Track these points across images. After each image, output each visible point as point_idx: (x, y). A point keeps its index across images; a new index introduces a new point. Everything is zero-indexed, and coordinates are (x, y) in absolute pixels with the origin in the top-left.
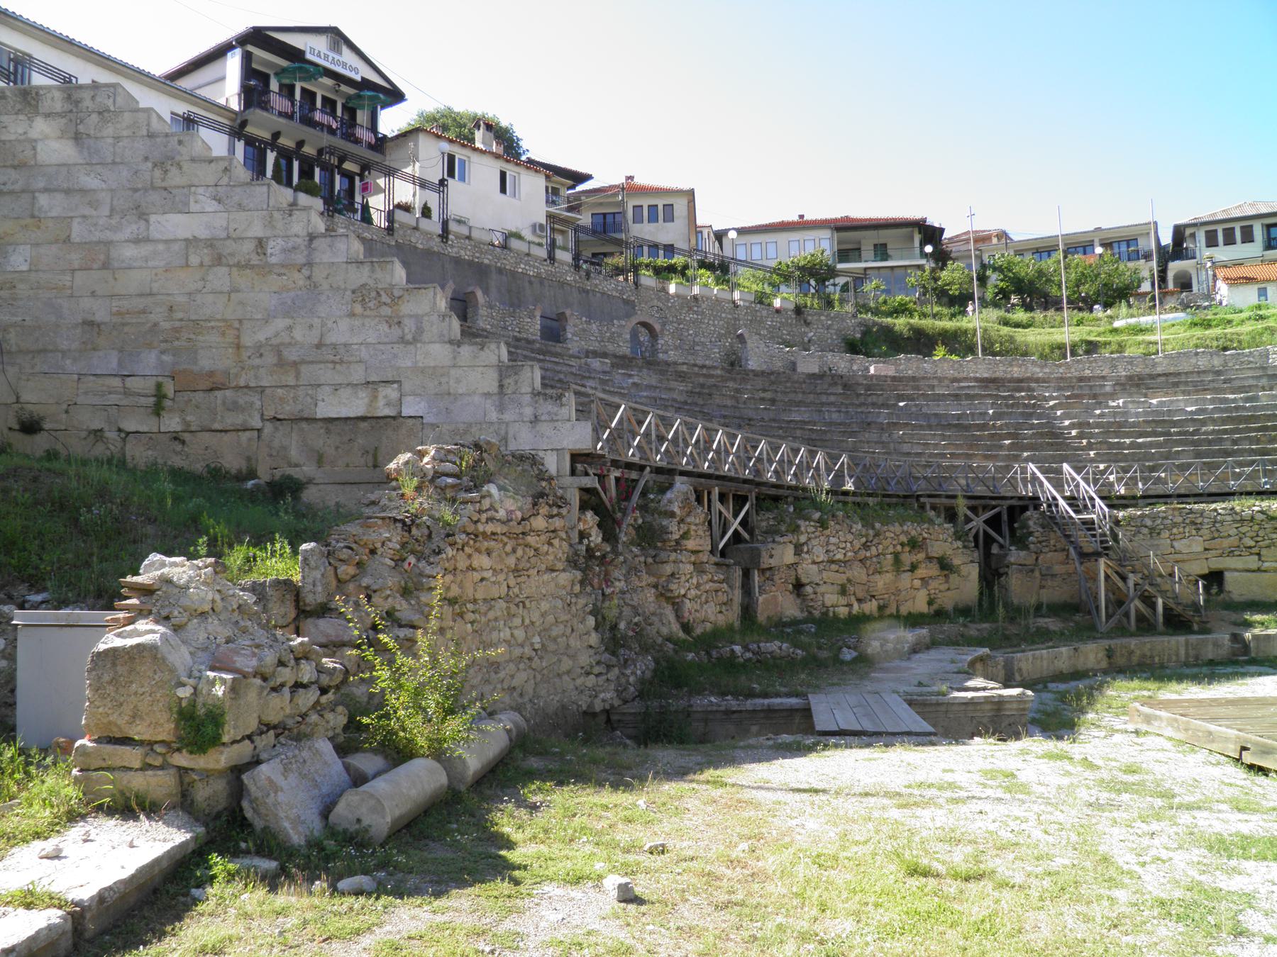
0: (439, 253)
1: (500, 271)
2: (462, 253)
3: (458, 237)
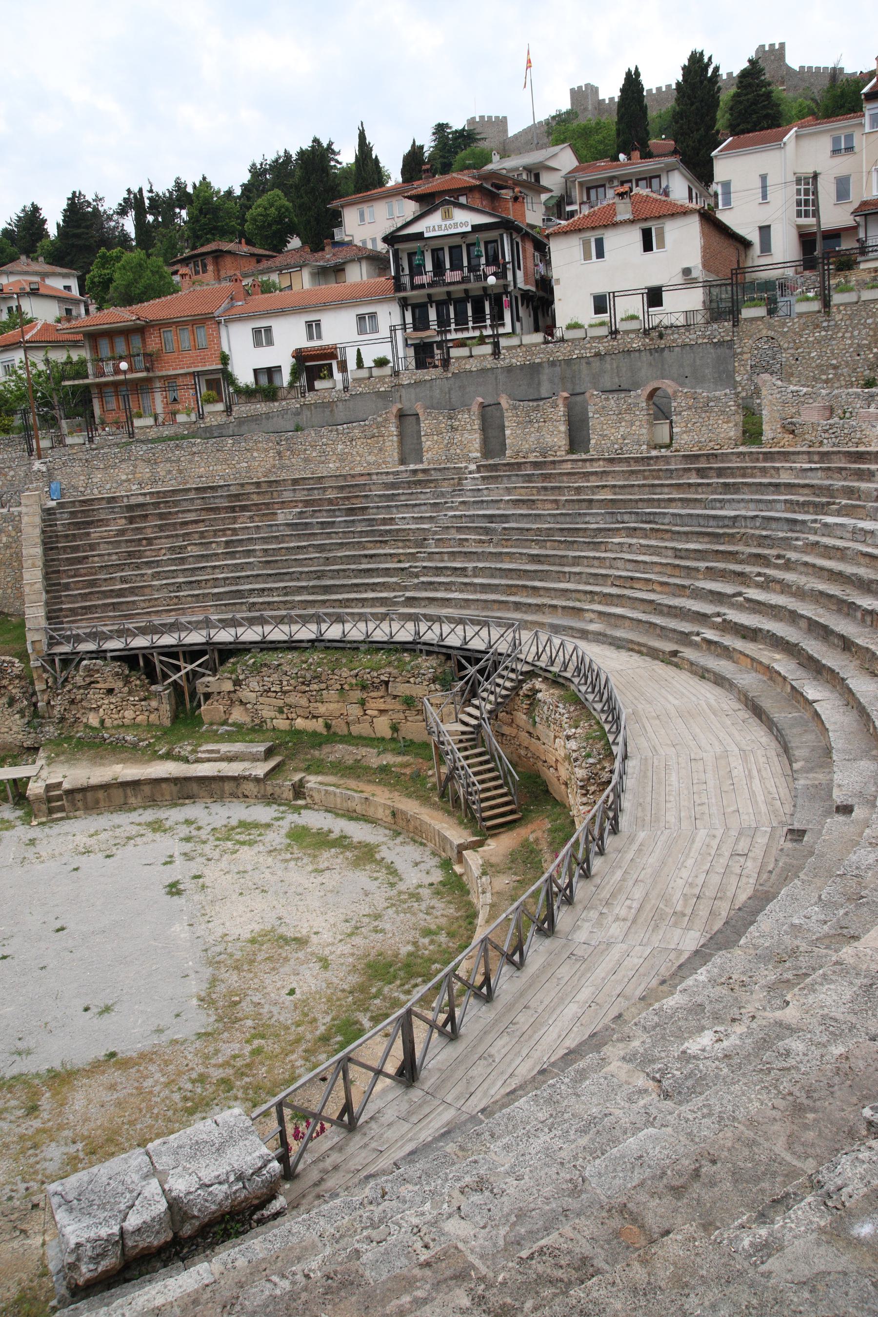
0: (492, 369)
1: (553, 364)
2: (514, 361)
3: (509, 348)
